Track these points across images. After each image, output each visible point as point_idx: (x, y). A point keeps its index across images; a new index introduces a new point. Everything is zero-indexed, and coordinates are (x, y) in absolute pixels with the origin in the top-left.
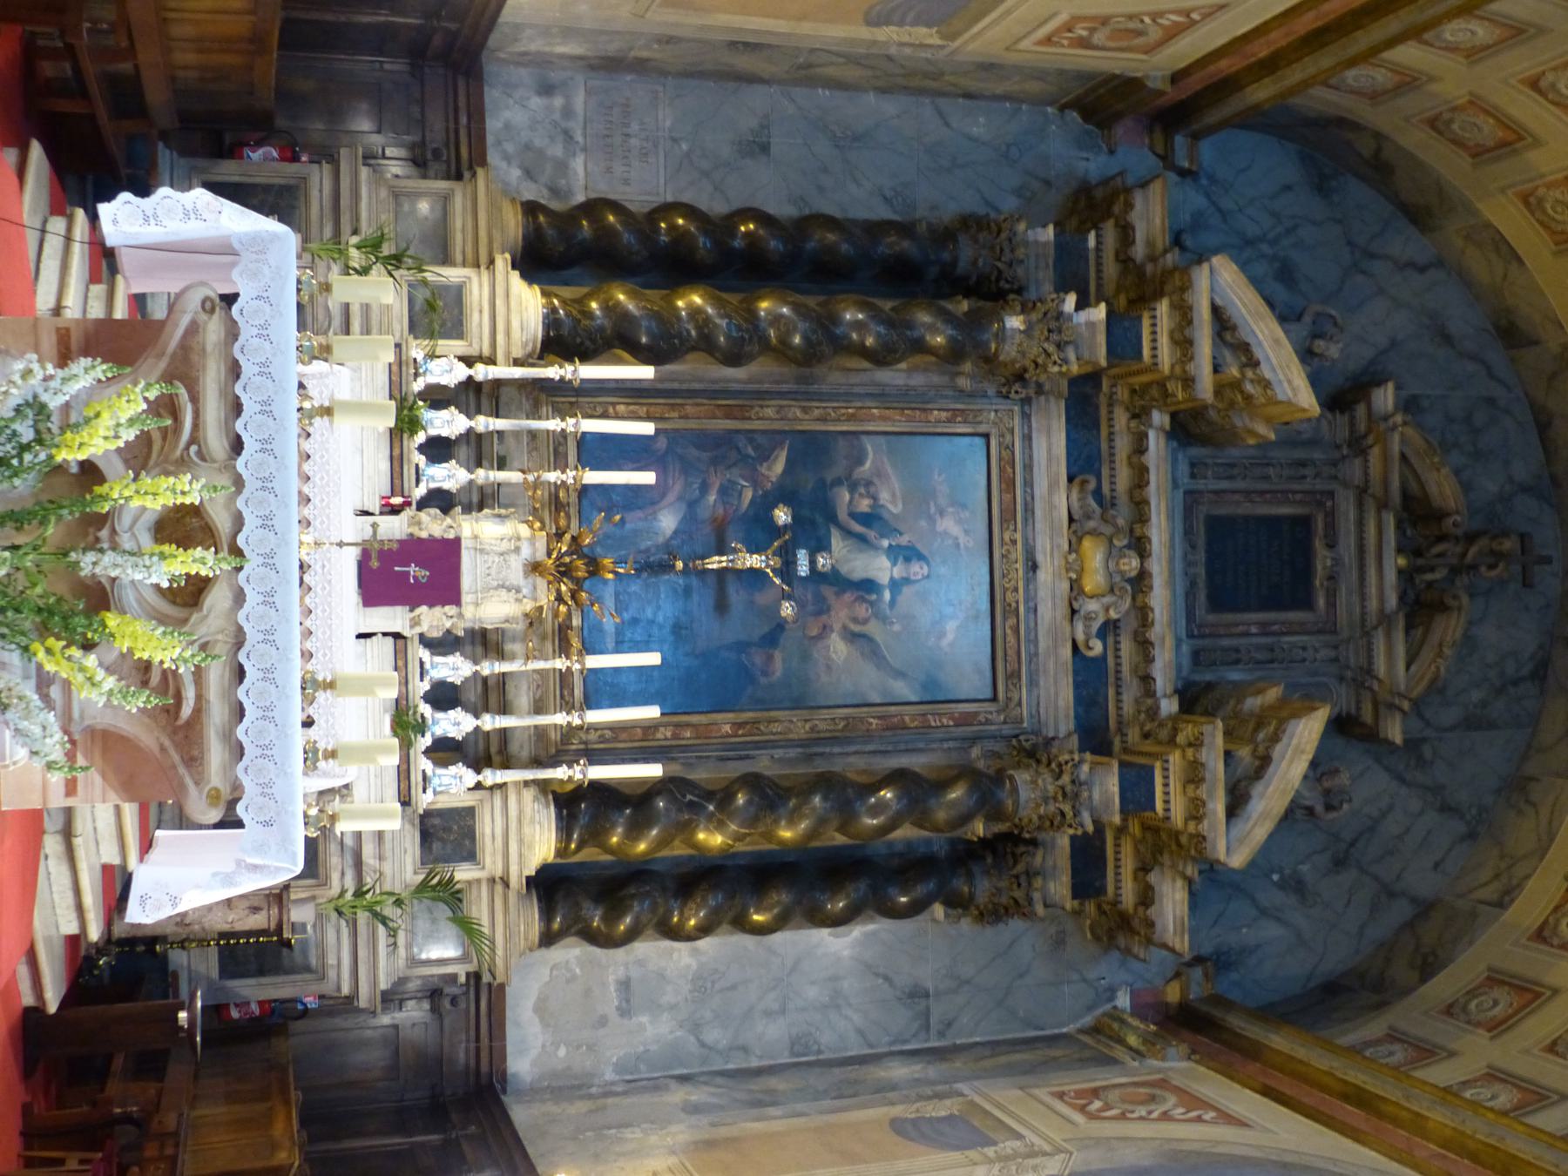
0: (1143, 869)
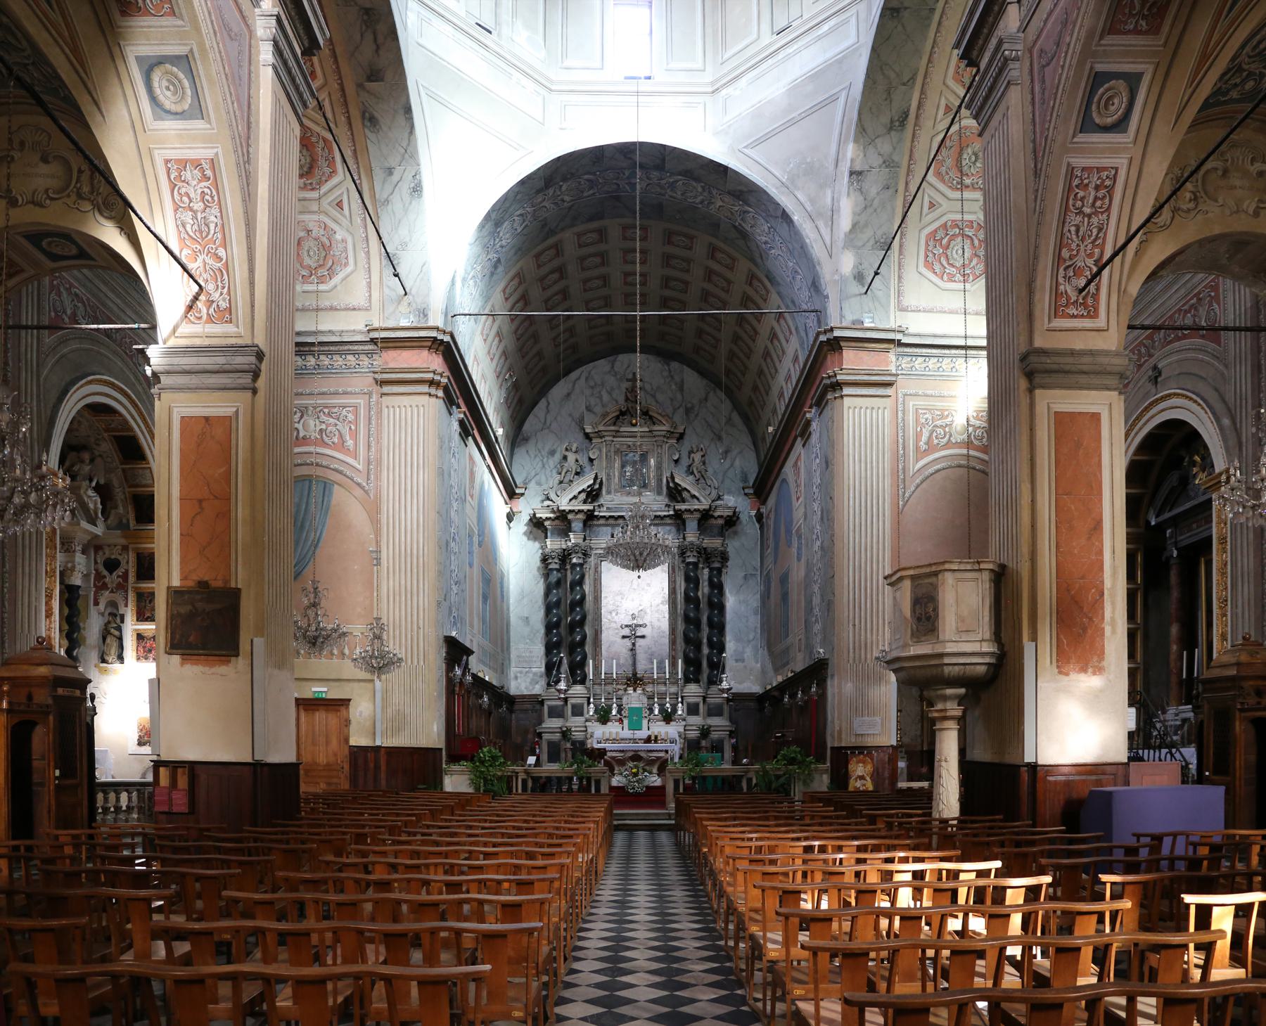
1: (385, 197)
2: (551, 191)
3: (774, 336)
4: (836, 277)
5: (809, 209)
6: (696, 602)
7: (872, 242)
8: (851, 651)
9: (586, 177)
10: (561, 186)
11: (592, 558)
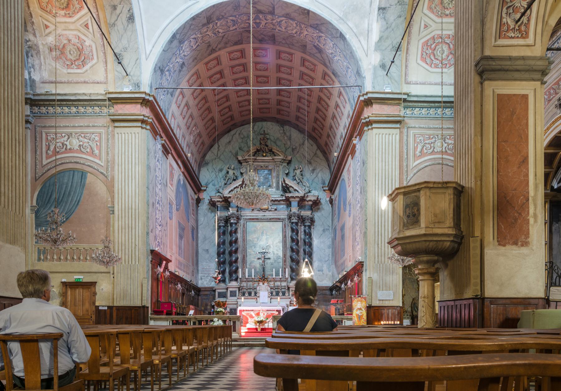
1: (113, 22)
2: (211, 26)
3: (337, 106)
5: (355, 31)
7: (391, 47)
9: (231, 18)
10: (217, 23)
11: (242, 221)
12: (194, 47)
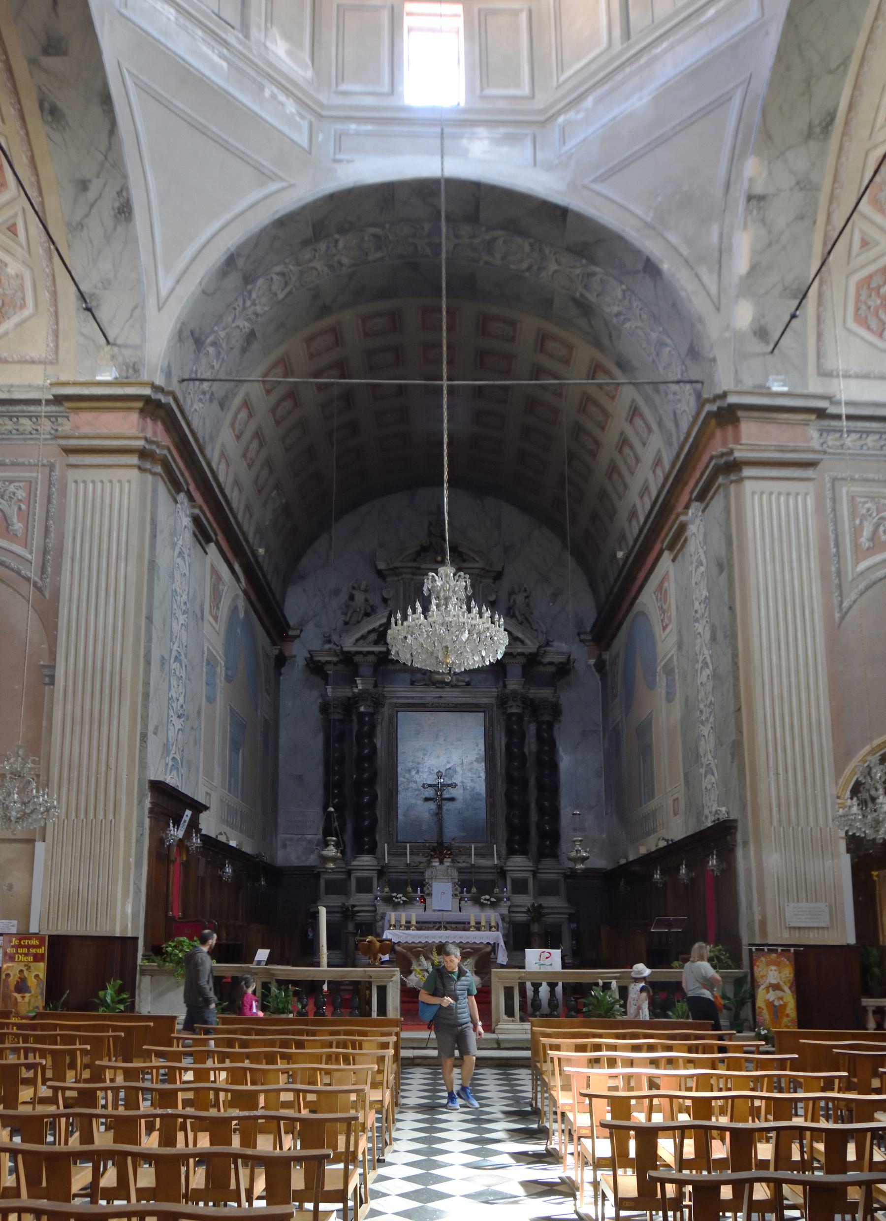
0: (545, 665)
2: (322, 246)
4: (727, 335)
6: (523, 758)
8: (775, 809)
9: (372, 230)
10: (337, 242)
11: (386, 708)
12: (281, 296)
